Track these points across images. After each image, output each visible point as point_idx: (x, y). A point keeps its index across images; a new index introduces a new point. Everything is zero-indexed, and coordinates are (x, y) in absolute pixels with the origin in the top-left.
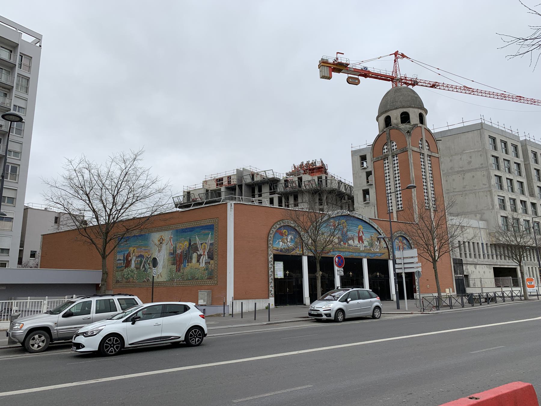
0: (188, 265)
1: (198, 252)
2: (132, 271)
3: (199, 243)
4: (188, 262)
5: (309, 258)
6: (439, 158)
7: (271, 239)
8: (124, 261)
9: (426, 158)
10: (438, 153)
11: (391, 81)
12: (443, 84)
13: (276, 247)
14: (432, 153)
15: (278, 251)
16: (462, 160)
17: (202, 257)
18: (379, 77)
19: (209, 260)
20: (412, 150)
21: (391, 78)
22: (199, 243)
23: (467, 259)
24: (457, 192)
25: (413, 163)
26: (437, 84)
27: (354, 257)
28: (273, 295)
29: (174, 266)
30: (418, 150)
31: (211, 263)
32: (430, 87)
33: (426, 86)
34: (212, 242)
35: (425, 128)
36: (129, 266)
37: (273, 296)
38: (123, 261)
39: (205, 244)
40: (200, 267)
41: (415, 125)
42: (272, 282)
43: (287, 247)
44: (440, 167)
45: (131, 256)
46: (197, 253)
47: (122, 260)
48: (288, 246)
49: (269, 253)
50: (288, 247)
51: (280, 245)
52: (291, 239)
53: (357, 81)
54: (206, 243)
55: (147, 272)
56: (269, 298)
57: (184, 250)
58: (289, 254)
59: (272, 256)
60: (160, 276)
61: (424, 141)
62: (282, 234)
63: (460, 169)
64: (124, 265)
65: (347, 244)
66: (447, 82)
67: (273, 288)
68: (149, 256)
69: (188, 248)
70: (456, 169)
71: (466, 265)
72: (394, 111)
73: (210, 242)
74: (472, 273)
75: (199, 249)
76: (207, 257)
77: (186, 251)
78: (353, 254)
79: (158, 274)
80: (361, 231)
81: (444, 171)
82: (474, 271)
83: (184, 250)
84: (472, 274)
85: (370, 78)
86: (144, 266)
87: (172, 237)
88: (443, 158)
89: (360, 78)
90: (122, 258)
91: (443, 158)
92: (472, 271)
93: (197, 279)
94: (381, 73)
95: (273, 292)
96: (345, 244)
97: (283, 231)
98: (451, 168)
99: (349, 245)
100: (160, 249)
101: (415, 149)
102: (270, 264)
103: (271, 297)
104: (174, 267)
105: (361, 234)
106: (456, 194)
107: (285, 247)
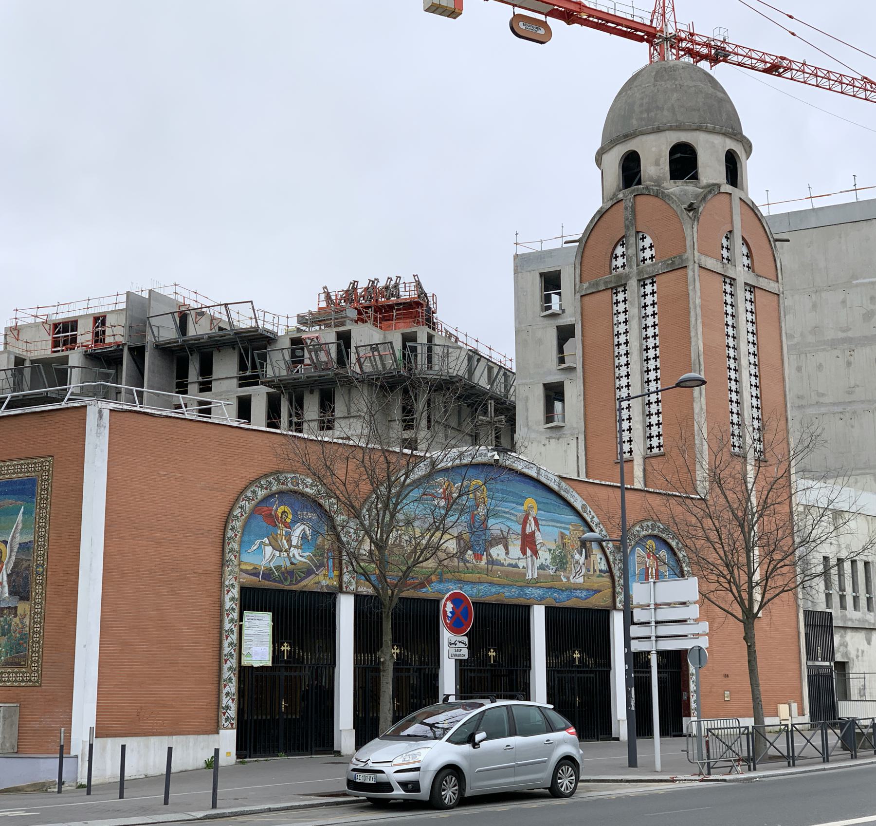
5: (359, 599)
6: (778, 295)
7: (236, 535)
9: (742, 295)
10: (777, 281)
11: (648, 41)
12: (804, 64)
13: (250, 564)
14: (761, 279)
15: (258, 577)
16: (848, 306)
18: (609, 24)
20: (700, 267)
21: (648, 34)
23: (846, 612)
24: (826, 405)
25: (702, 307)
26: (785, 63)
27: (506, 601)
28: (234, 722)
30: (718, 267)
31: (20, 611)
32: (765, 71)
33: (753, 68)
35: (740, 198)
37: (232, 724)
41: (713, 189)
42: (230, 679)
43: (288, 564)
44: (780, 323)
48: (293, 560)
49: (227, 583)
50: (292, 563)
51: (263, 557)
52: (304, 537)
53: (542, 31)
54: (5, 542)
56: (218, 733)
58: (294, 588)
59: (235, 592)
61: (738, 241)
62: (272, 520)
63: (841, 335)
65: (484, 557)
66: (815, 60)
67: (235, 697)
70: (830, 335)
71: (842, 631)
72: (652, 137)
73: (19, 539)
74: (857, 656)
78: (502, 590)
80: (531, 519)
81: (794, 337)
82: (863, 652)
84: (858, 661)
85: (582, 25)
88: (793, 296)
89: (552, 22)
91: (793, 296)
92: (858, 650)
94: (618, 14)
95: (233, 713)
96: (478, 557)
97: (277, 510)
98: (816, 330)
99: (492, 562)
101: (711, 263)
102: (226, 620)
103: (226, 728)
105: (531, 527)
106: (823, 410)
107: (282, 563)
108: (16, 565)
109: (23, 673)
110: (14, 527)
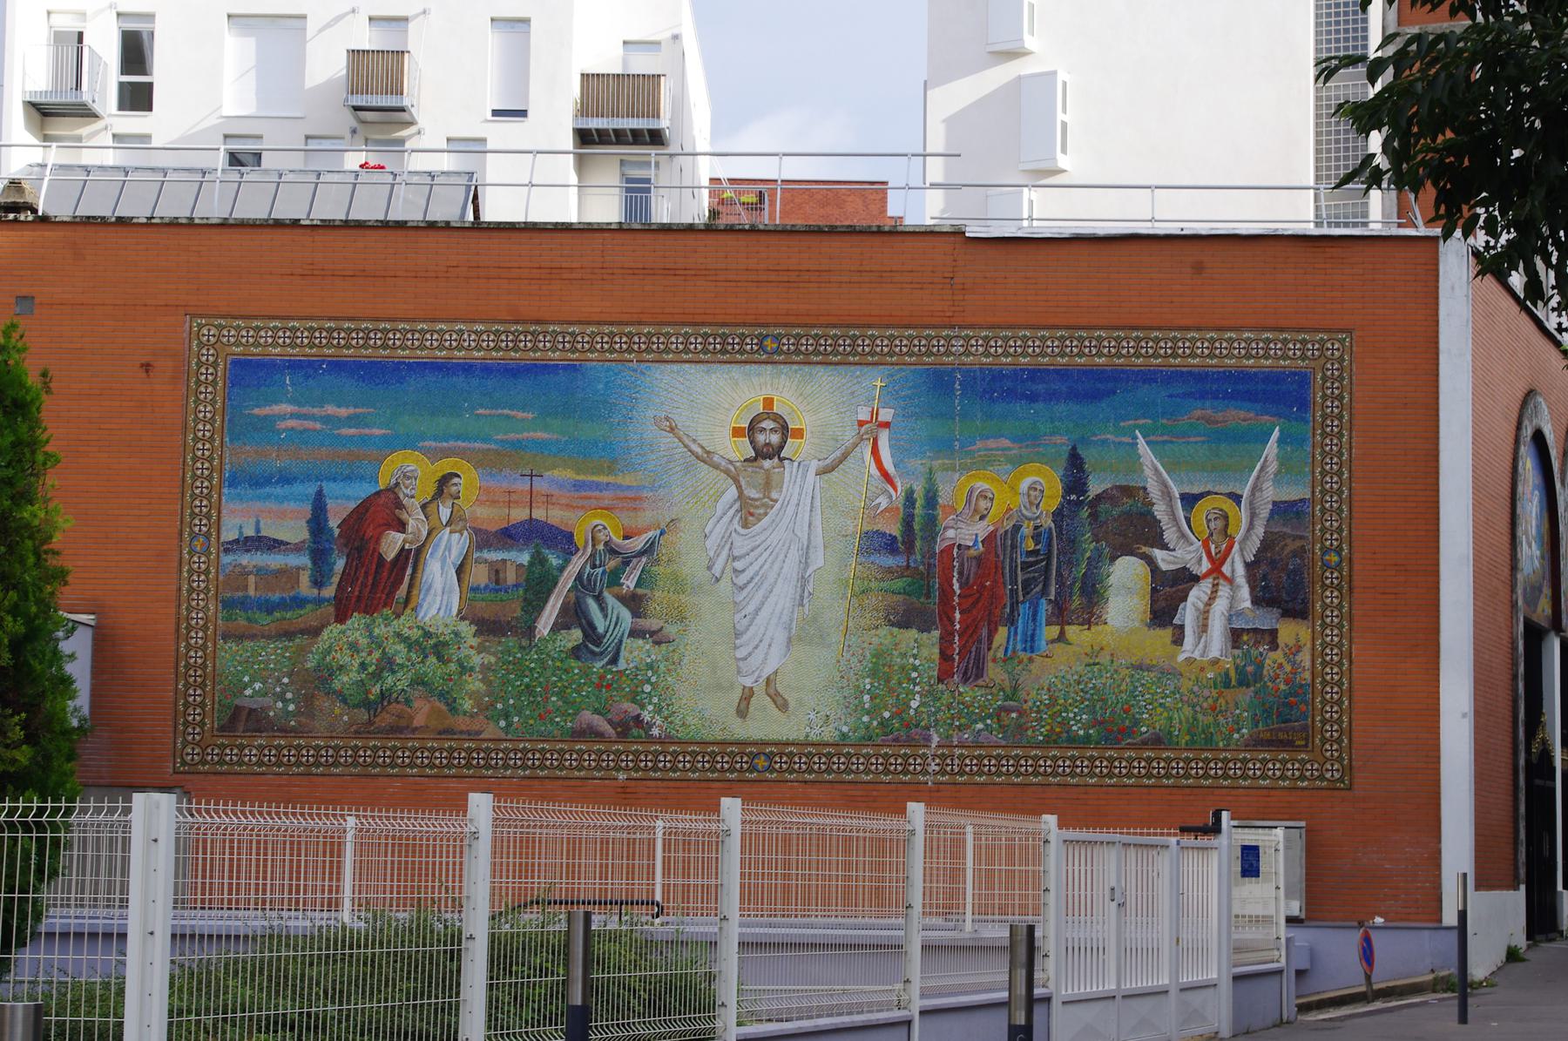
0: (1061, 637)
1: (1158, 554)
2: (434, 646)
3: (1167, 493)
4: (1061, 615)
8: (320, 557)
17: (1197, 595)
19: (1266, 619)
22: (1167, 493)
29: (913, 633)
34: (1296, 492)
36: (387, 603)
38: (304, 560)
39: (1228, 505)
40: (1181, 658)
45: (416, 522)
46: (1150, 561)
47: (298, 548)
54: (1237, 498)
55: (614, 660)
57: (1017, 528)
60: (761, 700)
64: (329, 592)
68: (638, 543)
69: (1058, 515)
73: (1270, 493)
75: (1170, 535)
76: (1245, 592)
77: (1036, 537)
79: (748, 682)
83: (1017, 528)
86: (573, 614)
87: (886, 415)
90: (295, 530)
93: (1157, 741)
100: (752, 493)
104: (922, 647)
108: (1267, 544)
109: (1302, 762)
110: (1258, 467)
